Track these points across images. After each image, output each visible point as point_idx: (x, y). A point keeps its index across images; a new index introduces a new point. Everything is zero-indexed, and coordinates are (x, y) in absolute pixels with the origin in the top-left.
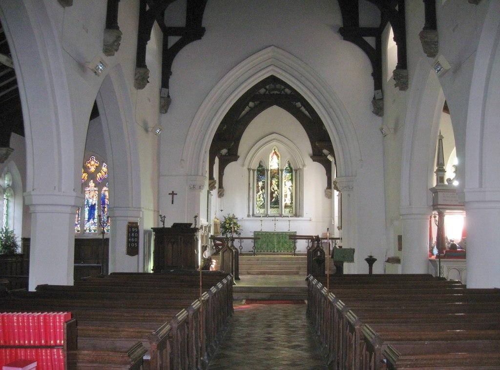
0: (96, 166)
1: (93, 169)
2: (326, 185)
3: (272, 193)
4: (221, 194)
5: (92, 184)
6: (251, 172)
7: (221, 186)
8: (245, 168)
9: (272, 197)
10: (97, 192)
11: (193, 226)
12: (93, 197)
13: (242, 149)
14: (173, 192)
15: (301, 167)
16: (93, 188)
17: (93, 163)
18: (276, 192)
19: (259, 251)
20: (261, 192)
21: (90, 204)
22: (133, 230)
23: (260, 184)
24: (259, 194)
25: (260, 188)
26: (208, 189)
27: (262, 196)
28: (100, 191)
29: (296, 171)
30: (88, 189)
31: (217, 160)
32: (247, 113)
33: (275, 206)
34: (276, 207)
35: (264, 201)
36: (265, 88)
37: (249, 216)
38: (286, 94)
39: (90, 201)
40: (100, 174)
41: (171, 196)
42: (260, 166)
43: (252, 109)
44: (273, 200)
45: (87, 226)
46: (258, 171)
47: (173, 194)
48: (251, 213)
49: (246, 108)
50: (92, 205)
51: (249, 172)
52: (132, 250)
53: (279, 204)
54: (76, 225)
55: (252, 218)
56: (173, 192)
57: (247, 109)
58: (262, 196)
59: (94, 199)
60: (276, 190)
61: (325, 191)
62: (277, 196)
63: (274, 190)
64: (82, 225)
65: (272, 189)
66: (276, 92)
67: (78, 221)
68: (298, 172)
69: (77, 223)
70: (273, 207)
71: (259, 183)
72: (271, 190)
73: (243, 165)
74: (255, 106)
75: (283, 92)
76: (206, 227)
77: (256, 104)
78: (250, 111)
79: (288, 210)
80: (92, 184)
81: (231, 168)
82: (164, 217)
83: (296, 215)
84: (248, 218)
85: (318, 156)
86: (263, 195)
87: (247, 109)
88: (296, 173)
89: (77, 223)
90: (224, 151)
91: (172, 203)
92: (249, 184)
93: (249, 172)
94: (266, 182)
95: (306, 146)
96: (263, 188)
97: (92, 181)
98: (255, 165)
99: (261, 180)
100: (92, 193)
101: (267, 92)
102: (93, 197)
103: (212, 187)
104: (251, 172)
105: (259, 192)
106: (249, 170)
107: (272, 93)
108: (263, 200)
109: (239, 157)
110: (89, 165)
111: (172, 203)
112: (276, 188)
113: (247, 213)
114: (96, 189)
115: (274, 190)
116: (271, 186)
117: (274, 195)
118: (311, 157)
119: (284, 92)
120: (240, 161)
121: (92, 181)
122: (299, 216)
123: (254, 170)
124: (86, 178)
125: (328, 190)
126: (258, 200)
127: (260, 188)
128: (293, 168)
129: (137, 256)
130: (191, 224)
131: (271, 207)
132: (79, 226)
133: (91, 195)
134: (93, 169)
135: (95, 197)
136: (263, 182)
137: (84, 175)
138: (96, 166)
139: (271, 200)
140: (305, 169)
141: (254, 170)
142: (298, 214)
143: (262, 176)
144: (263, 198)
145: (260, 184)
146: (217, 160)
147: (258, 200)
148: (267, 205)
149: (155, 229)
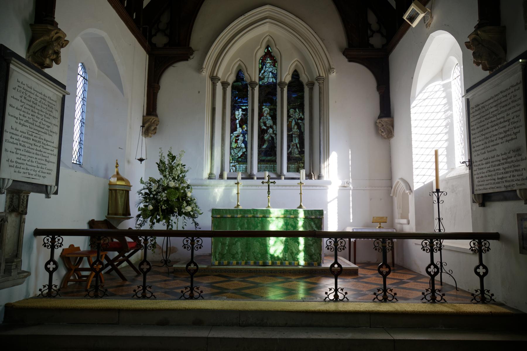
3: (262, 132)
18: (270, 131)
19: (225, 262)
20: (239, 130)
23: (239, 114)
25: (237, 121)
27: (241, 138)
29: (311, 85)
33: (269, 158)
35: (246, 147)
44: (265, 146)
46: (234, 88)
53: (275, 155)
58: (241, 138)
60: (271, 127)
62: (272, 138)
63: (265, 125)
65: (262, 124)
71: (237, 113)
72: (260, 127)
79: (293, 166)
86: (244, 136)
94: (249, 108)
96: (244, 122)
99: (240, 107)
104: (219, 87)
108: (243, 145)
112: (269, 122)
115: (265, 125)
116: (259, 119)
117: (266, 137)
125: (385, 119)
126: (234, 145)
127: (237, 121)
131: (260, 161)
136: (243, 110)
139: (260, 146)
140: (333, 76)
141: (225, 84)
143: (243, 98)
144: (245, 142)
145: (239, 114)
147: (234, 145)
148: (252, 154)
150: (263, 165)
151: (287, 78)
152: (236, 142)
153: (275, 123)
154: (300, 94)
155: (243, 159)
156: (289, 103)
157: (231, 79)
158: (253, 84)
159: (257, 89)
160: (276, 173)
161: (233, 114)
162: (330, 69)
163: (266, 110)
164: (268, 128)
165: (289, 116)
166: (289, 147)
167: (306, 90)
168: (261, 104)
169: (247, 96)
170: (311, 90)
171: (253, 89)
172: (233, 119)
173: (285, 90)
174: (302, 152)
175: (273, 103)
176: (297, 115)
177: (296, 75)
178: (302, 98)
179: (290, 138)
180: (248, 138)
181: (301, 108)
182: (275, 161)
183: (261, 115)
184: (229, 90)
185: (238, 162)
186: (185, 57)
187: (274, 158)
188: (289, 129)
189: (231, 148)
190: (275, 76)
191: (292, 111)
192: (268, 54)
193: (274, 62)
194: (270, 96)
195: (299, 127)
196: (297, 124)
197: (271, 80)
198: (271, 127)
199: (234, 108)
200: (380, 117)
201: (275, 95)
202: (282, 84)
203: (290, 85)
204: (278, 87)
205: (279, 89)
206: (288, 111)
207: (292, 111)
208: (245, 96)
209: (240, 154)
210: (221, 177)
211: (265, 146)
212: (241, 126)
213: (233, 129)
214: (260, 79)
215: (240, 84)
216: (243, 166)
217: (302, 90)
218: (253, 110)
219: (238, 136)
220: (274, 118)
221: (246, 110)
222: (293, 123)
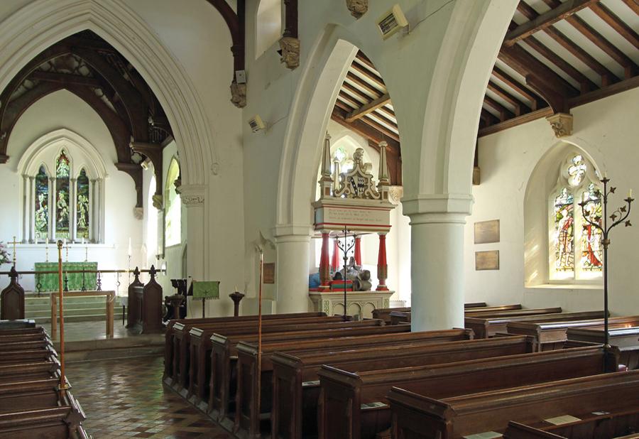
2: (135, 202)
3: (59, 211)
6: (28, 180)
8: (20, 172)
9: (59, 217)
13: (11, 149)
15: (101, 177)
18: (65, 210)
20: (42, 209)
23: (41, 198)
24: (39, 211)
25: (40, 203)
27: (43, 214)
29: (94, 182)
32: (23, 95)
34: (65, 230)
36: (50, 63)
38: (81, 75)
42: (41, 171)
43: (28, 90)
44: (61, 220)
46: (37, 179)
48: (27, 238)
49: (19, 87)
51: (25, 180)
53: (68, 227)
55: (28, 245)
57: (21, 90)
60: (65, 207)
61: (134, 210)
66: (65, 71)
68: (97, 183)
70: (60, 230)
71: (40, 197)
72: (57, 207)
73: (15, 169)
74: (35, 87)
75: (76, 71)
77: (36, 84)
79: (81, 234)
83: (93, 241)
85: (126, 163)
86: (45, 213)
88: (94, 184)
92: (25, 197)
93: (25, 180)
95: (108, 148)
96: (45, 203)
98: (33, 171)
99: (42, 193)
101: (53, 69)
105: (39, 208)
106: (24, 176)
107: (60, 70)
108: (45, 220)
109: (8, 157)
112: (64, 204)
115: (61, 205)
116: (57, 201)
117: (62, 214)
118: (115, 164)
119: (78, 71)
120: (10, 162)
122: (98, 243)
123: (31, 178)
127: (40, 203)
128: (90, 179)
131: (57, 230)
139: (57, 221)
140: (107, 179)
141: (31, 178)
142: (96, 240)
143: (44, 186)
145: (41, 198)
147: (38, 219)
148: (52, 226)
150: (60, 233)
151: (76, 175)
152: (40, 216)
153: (68, 205)
154: (86, 185)
155: (45, 229)
156: (78, 192)
157: (35, 173)
158: (52, 179)
159: (55, 182)
160: (69, 239)
161: (37, 197)
162: (106, 175)
163: (62, 195)
164: (63, 208)
165: (78, 200)
166: (78, 221)
167: (90, 184)
168: (58, 191)
169: (47, 186)
170: (94, 184)
171: (52, 182)
172: (37, 201)
173: (76, 183)
174: (87, 225)
175: (67, 191)
176: (84, 199)
177: (83, 172)
178: (88, 188)
179: (79, 215)
180: (49, 214)
181: (87, 194)
182: (68, 231)
183: (58, 198)
184: (34, 181)
185: (41, 231)
186: (4, 162)
187: (66, 228)
188: (78, 209)
189: (36, 221)
190: (68, 172)
191: (80, 196)
192: (63, 156)
193: (68, 162)
194: (65, 186)
195: (85, 208)
196: (84, 206)
197: (65, 175)
198: (65, 207)
199: (37, 193)
200: (136, 207)
201: (68, 185)
202: (73, 180)
203: (79, 179)
204: (70, 181)
205: (71, 182)
206: (78, 197)
207: (80, 196)
208: (46, 185)
209: (43, 225)
210: (31, 241)
211: (61, 220)
212: (43, 206)
213: (38, 208)
214: (57, 174)
215: (42, 176)
216: (45, 234)
217: (87, 183)
218: (52, 197)
219: (41, 213)
220: (67, 201)
221: (47, 195)
222: (81, 205)
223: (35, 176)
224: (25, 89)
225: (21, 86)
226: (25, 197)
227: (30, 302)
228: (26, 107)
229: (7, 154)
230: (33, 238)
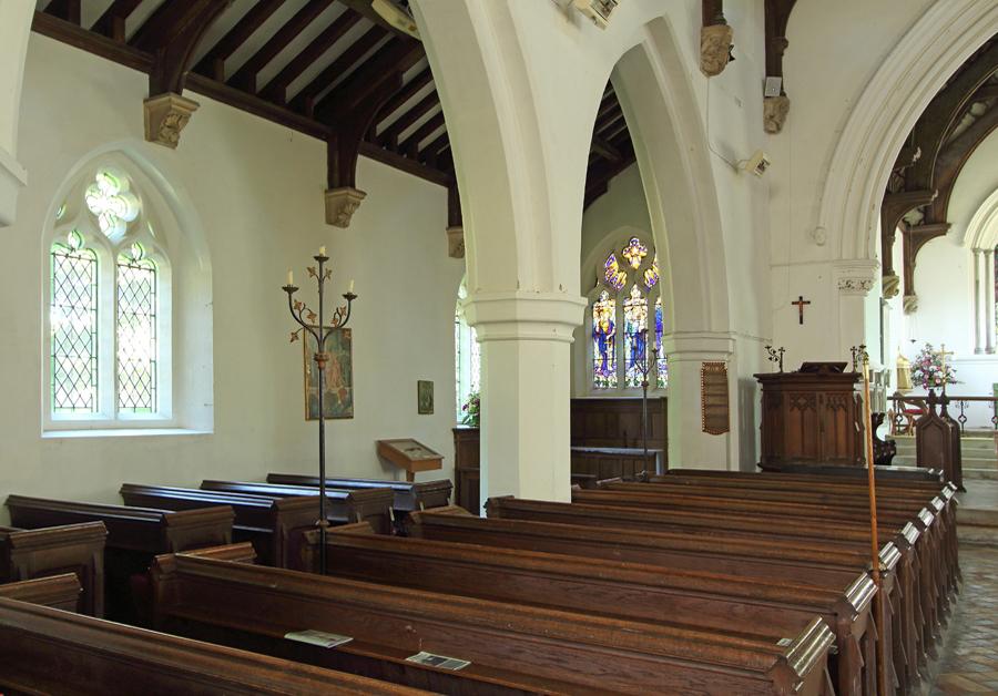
0: (642, 257)
1: (636, 263)
4: (909, 308)
5: (636, 292)
6: (982, 256)
7: (909, 291)
10: (645, 307)
11: (847, 370)
12: (639, 317)
13: (955, 210)
14: (801, 298)
16: (638, 300)
17: (635, 250)
21: (634, 331)
22: (714, 377)
26: (881, 295)
28: (651, 305)
30: (629, 303)
31: (899, 234)
32: (969, 128)
37: (977, 351)
39: (635, 325)
40: (649, 271)
41: (797, 307)
43: (978, 118)
45: (630, 373)
47: (801, 302)
48: (983, 345)
49: (964, 117)
50: (637, 333)
51: (976, 256)
52: (715, 422)
54: (610, 372)
55: (983, 355)
56: (801, 298)
57: (967, 120)
59: (642, 322)
64: (622, 372)
67: (612, 366)
69: (611, 369)
73: (960, 242)
74: (988, 111)
76: (879, 375)
78: (973, 124)
80: (636, 292)
81: (930, 252)
82: (782, 350)
84: (977, 356)
87: (967, 120)
89: (611, 369)
90: (914, 216)
91: (801, 322)
92: (977, 282)
93: (976, 256)
97: (635, 286)
100: (637, 310)
102: (639, 317)
103: (889, 290)
106: (975, 251)
109: (949, 225)
110: (628, 256)
111: (801, 322)
113: (973, 347)
114: (643, 301)
120: (952, 233)
121: (635, 286)
123: (987, 252)
124: (624, 282)
129: (725, 434)
130: (844, 365)
132: (614, 374)
133: (636, 314)
134: (636, 263)
135: (643, 317)
137: (621, 274)
138: (642, 257)
141: (987, 252)
146: (899, 234)
149: (762, 378)
184: (992, 256)
223: (993, 248)
224: (973, 119)
225: (967, 116)
226: (977, 282)
227: (981, 444)
228: (974, 145)
229: (948, 221)
230: (993, 344)
